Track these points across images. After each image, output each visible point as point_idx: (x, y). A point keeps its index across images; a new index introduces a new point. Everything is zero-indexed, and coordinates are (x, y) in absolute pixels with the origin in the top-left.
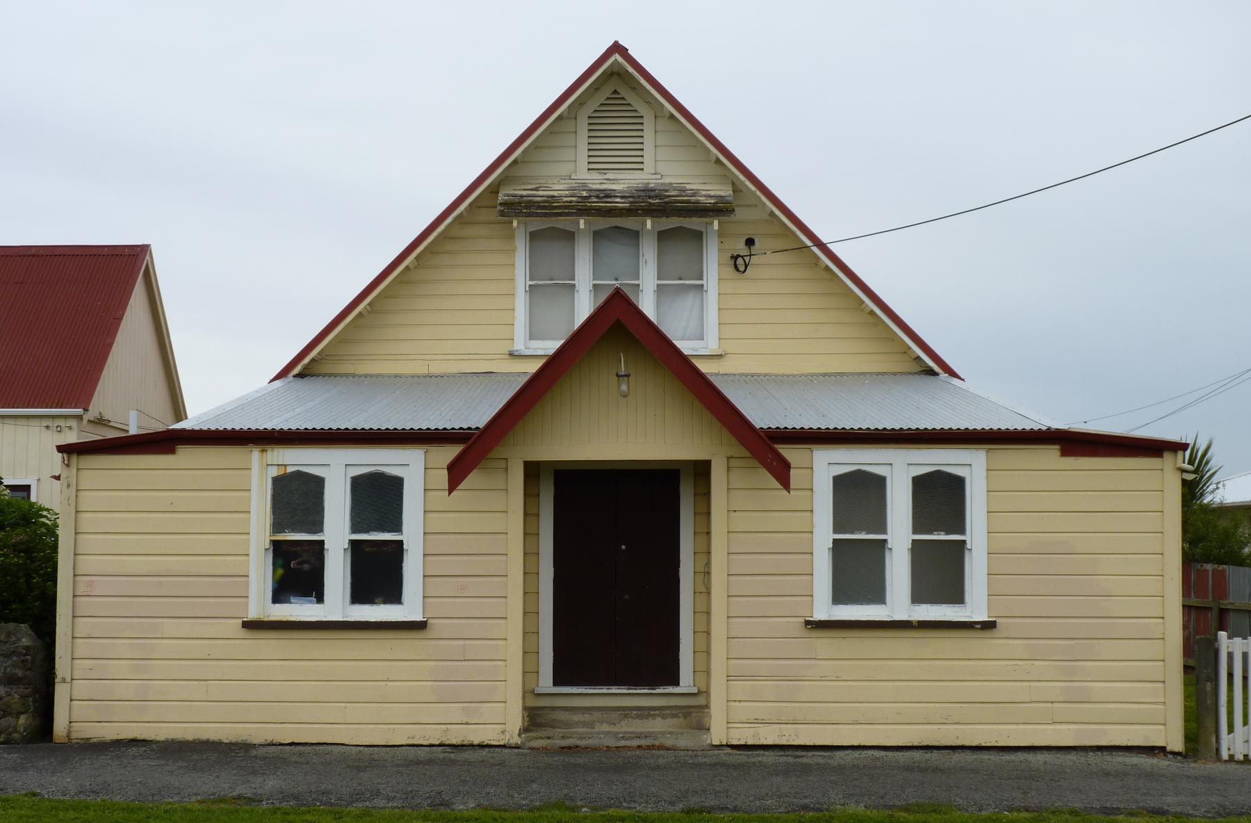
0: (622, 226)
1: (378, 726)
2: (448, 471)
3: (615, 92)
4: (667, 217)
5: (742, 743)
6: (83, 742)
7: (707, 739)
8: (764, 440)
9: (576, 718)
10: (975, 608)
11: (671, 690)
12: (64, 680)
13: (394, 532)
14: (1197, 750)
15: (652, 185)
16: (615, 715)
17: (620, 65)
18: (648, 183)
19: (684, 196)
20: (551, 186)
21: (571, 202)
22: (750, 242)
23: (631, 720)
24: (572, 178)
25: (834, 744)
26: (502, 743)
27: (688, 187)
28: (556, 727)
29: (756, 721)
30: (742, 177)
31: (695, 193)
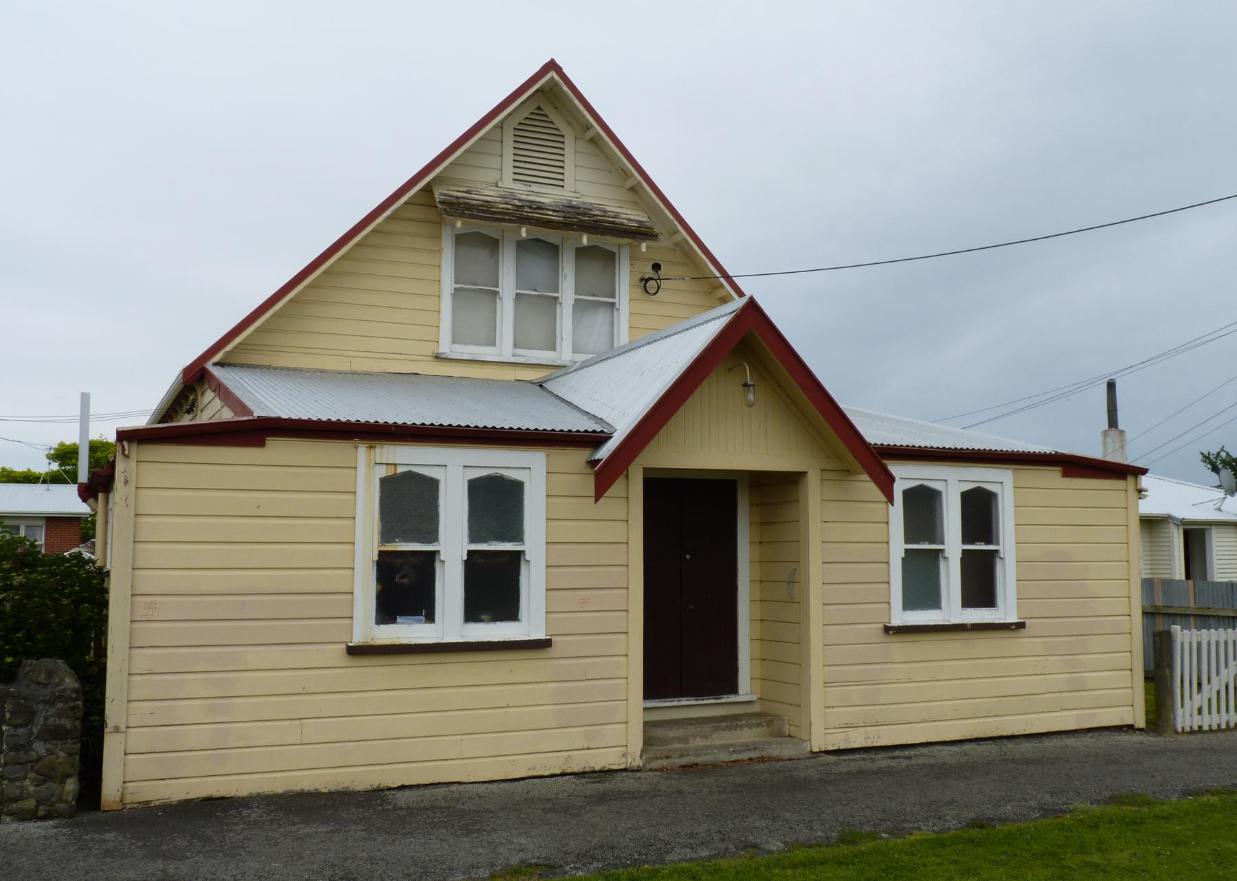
0: (544, 239)
1: (497, 758)
2: (595, 477)
3: (539, 108)
4: (602, 235)
5: (836, 747)
6: (140, 806)
7: (807, 746)
8: (874, 455)
9: (671, 733)
10: (1005, 612)
11: (733, 698)
12: (117, 730)
13: (516, 541)
14: (1159, 725)
15: (575, 203)
16: (707, 728)
17: (556, 84)
18: (571, 201)
19: (607, 217)
20: (482, 191)
21: (508, 209)
22: (656, 267)
23: (722, 732)
24: (499, 185)
25: (909, 743)
26: (623, 767)
27: (608, 208)
28: (653, 745)
29: (847, 726)
30: (662, 205)
31: (616, 216)
